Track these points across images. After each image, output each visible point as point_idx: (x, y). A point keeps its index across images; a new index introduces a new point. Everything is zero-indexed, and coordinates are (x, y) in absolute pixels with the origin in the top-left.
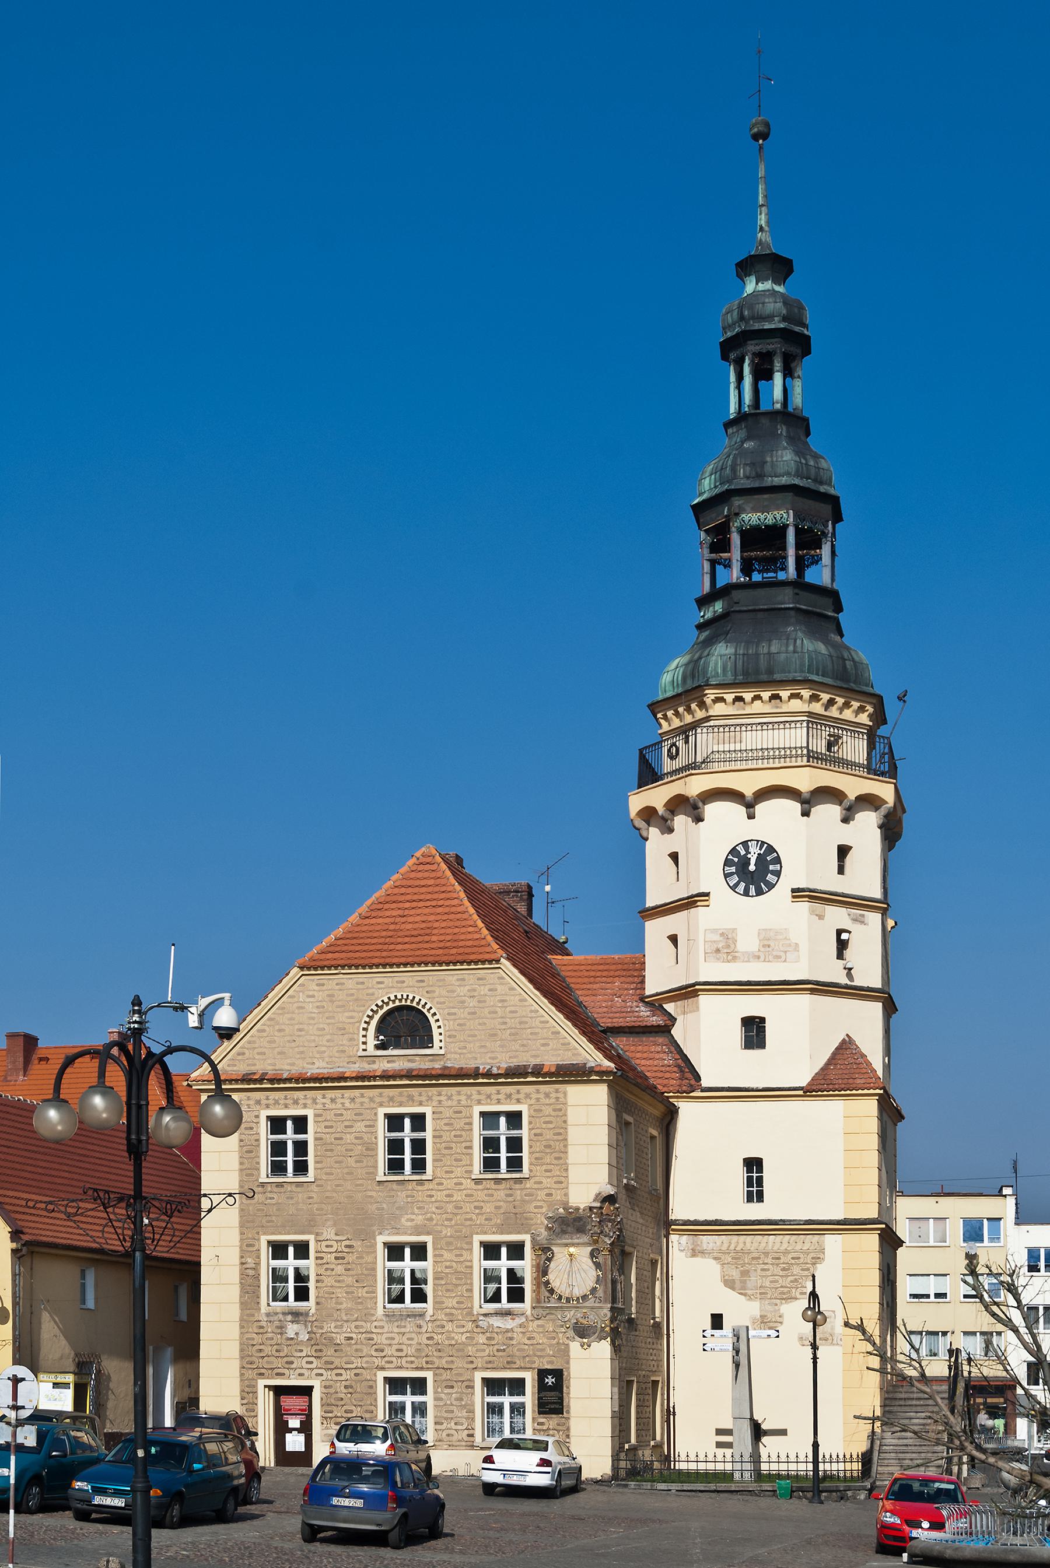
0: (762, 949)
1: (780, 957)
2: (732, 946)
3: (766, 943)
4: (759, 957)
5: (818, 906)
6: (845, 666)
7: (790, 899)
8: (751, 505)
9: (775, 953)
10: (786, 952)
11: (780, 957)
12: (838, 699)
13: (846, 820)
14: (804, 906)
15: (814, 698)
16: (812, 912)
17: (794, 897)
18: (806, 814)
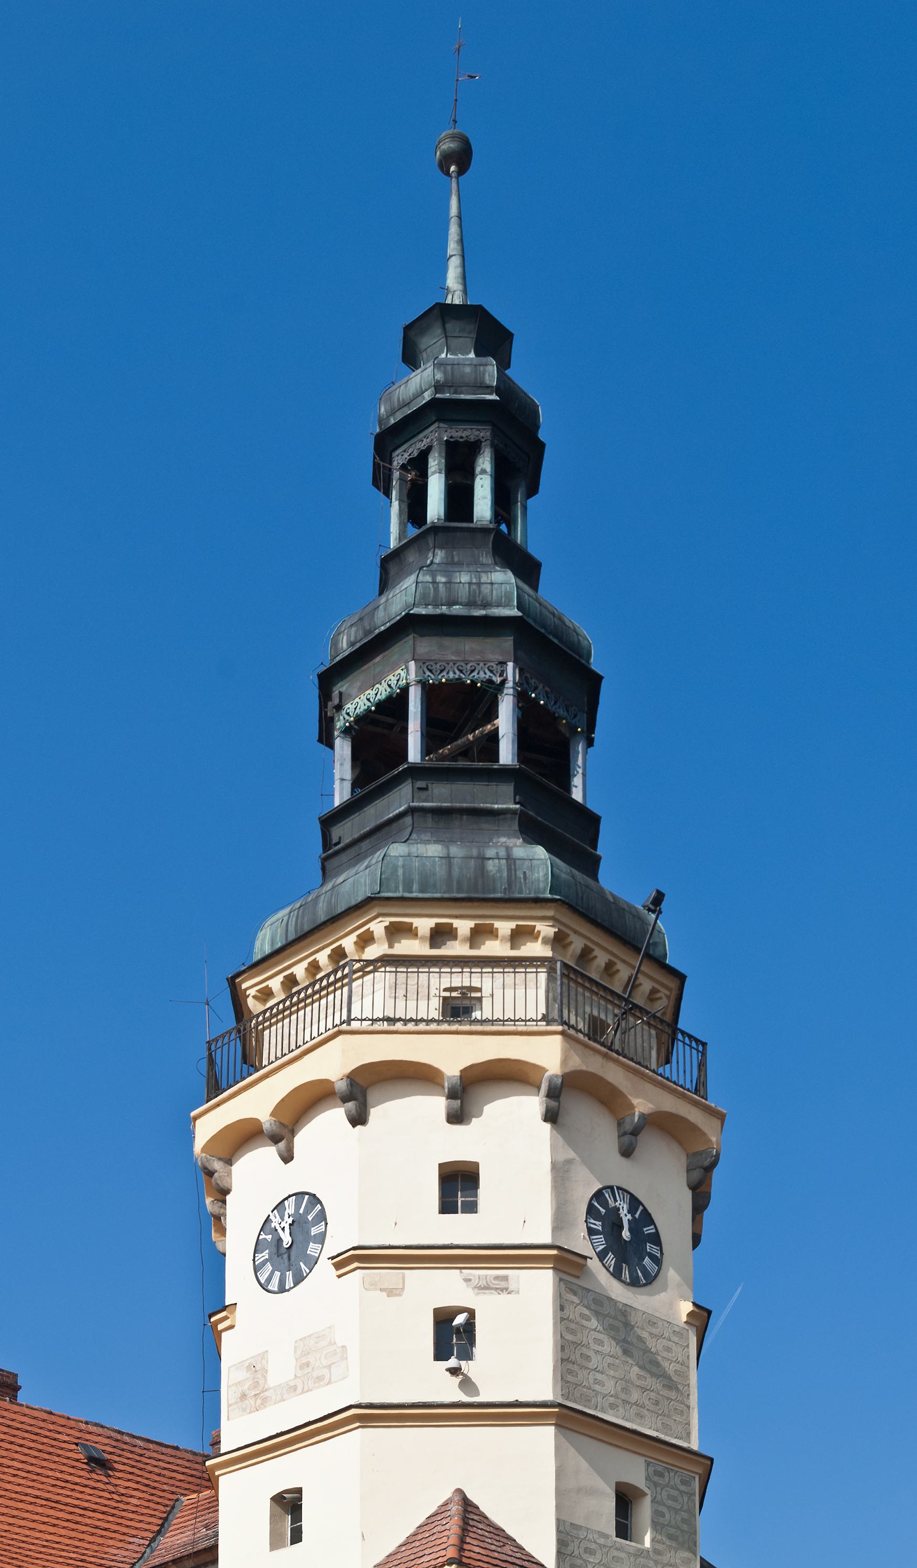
0: (299, 1374)
1: (320, 1379)
2: (261, 1382)
3: (304, 1360)
4: (295, 1388)
5: (387, 1276)
6: (482, 869)
7: (334, 1272)
8: (358, 684)
9: (315, 1374)
10: (329, 1367)
11: (320, 1379)
12: (456, 923)
13: (457, 1117)
14: (357, 1277)
15: (395, 932)
16: (368, 1286)
17: (338, 1266)
18: (358, 1119)
